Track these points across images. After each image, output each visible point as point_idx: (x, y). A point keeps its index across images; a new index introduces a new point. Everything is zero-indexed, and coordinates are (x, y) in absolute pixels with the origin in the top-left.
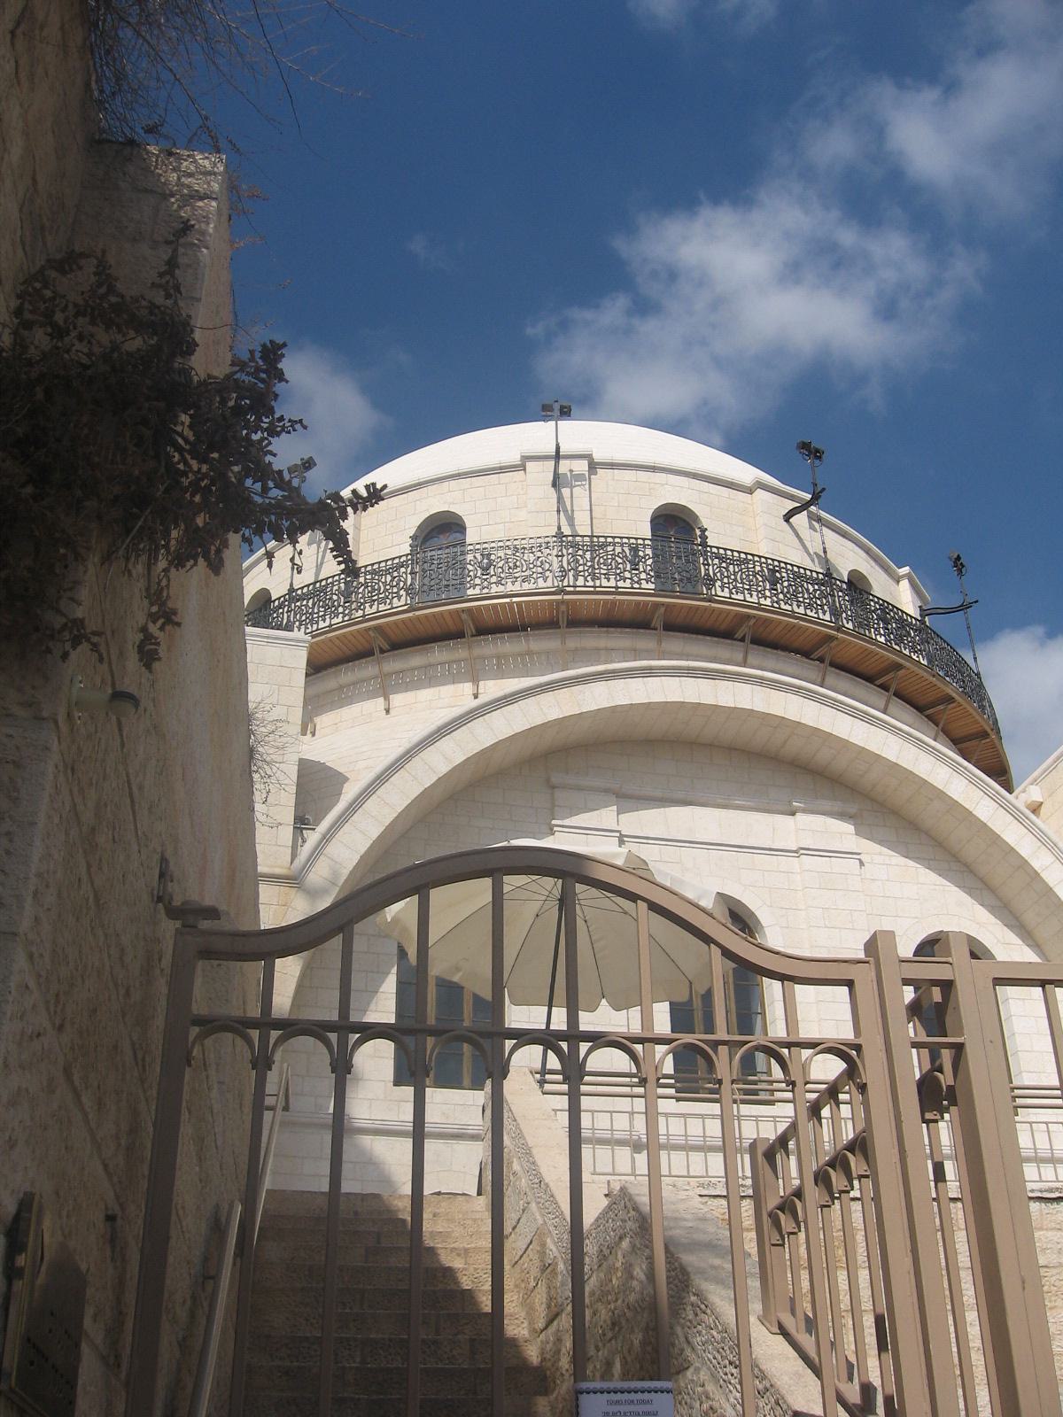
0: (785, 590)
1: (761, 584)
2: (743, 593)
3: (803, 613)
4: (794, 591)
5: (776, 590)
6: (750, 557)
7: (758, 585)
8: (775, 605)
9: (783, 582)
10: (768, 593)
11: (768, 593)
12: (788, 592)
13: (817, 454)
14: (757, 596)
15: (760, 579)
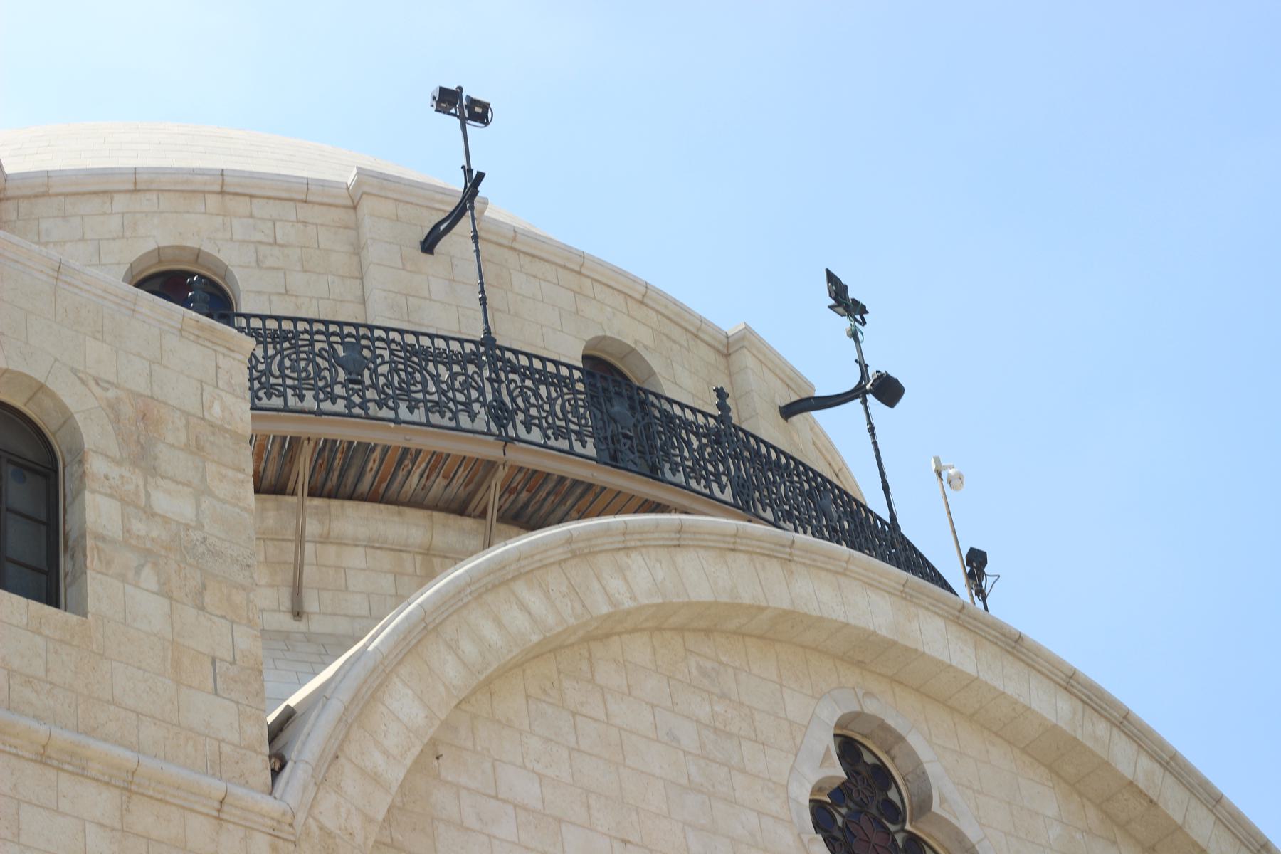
0: (382, 380)
1: (326, 373)
2: (284, 395)
3: (424, 420)
4: (401, 381)
5: (361, 382)
6: (302, 326)
7: (318, 375)
8: (357, 411)
9: (377, 366)
10: (339, 390)
11: (339, 390)
12: (389, 384)
13: (478, 113)
14: (316, 397)
15: (323, 364)
